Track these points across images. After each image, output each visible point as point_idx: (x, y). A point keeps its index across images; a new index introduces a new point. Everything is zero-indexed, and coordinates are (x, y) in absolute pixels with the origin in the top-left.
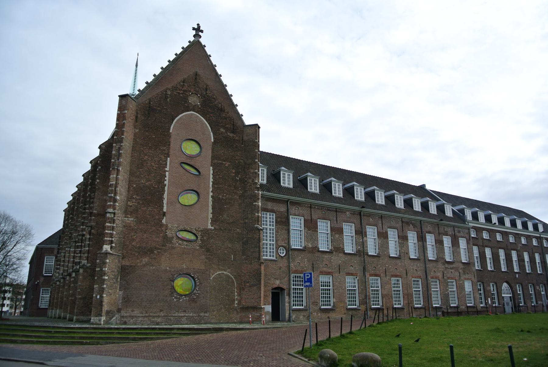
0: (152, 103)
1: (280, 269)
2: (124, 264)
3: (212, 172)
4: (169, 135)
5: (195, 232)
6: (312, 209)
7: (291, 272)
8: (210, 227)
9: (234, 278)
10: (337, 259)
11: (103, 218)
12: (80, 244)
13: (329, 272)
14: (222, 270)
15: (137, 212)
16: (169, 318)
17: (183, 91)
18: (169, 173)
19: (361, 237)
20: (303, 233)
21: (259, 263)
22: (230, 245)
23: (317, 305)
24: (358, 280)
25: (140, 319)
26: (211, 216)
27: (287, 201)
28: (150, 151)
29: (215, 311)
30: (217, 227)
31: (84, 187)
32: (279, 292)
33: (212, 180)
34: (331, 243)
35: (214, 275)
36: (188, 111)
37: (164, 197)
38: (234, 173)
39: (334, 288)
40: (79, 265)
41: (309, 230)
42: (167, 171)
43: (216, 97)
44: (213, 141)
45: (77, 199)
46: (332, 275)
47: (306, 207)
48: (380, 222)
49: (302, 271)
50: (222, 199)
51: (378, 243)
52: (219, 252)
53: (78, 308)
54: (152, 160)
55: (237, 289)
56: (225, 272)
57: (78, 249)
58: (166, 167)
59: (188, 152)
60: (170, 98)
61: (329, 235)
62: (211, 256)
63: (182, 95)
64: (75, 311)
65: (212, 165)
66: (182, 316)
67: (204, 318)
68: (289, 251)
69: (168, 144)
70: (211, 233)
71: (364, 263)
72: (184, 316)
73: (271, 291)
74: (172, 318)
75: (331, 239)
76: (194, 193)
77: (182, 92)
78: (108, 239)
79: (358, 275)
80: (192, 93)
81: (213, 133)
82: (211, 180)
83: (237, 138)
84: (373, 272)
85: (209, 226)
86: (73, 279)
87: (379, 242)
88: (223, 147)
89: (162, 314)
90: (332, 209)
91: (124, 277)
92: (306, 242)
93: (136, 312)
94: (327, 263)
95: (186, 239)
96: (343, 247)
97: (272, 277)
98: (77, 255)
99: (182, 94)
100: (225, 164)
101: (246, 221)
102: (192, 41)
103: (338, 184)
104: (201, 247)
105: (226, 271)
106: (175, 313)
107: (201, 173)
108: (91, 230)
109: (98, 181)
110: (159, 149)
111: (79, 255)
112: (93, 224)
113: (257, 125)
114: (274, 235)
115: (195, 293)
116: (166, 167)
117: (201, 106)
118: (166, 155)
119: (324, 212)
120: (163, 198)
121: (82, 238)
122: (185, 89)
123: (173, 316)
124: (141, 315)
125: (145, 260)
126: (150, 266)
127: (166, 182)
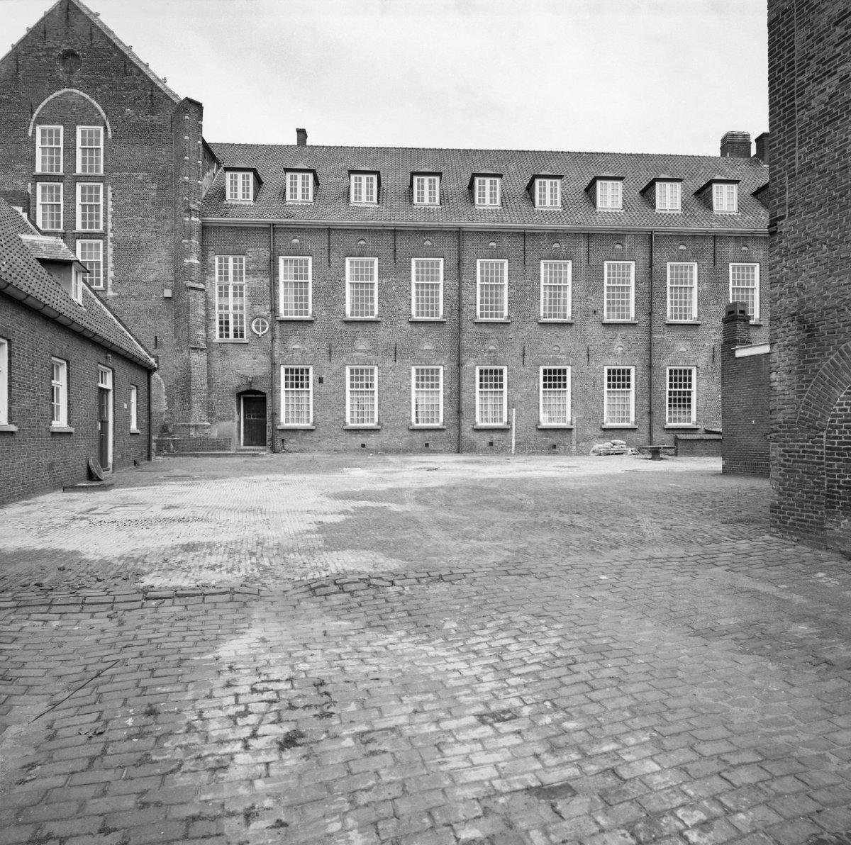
38: (154, 190)
88: (132, 144)
99: (44, 56)
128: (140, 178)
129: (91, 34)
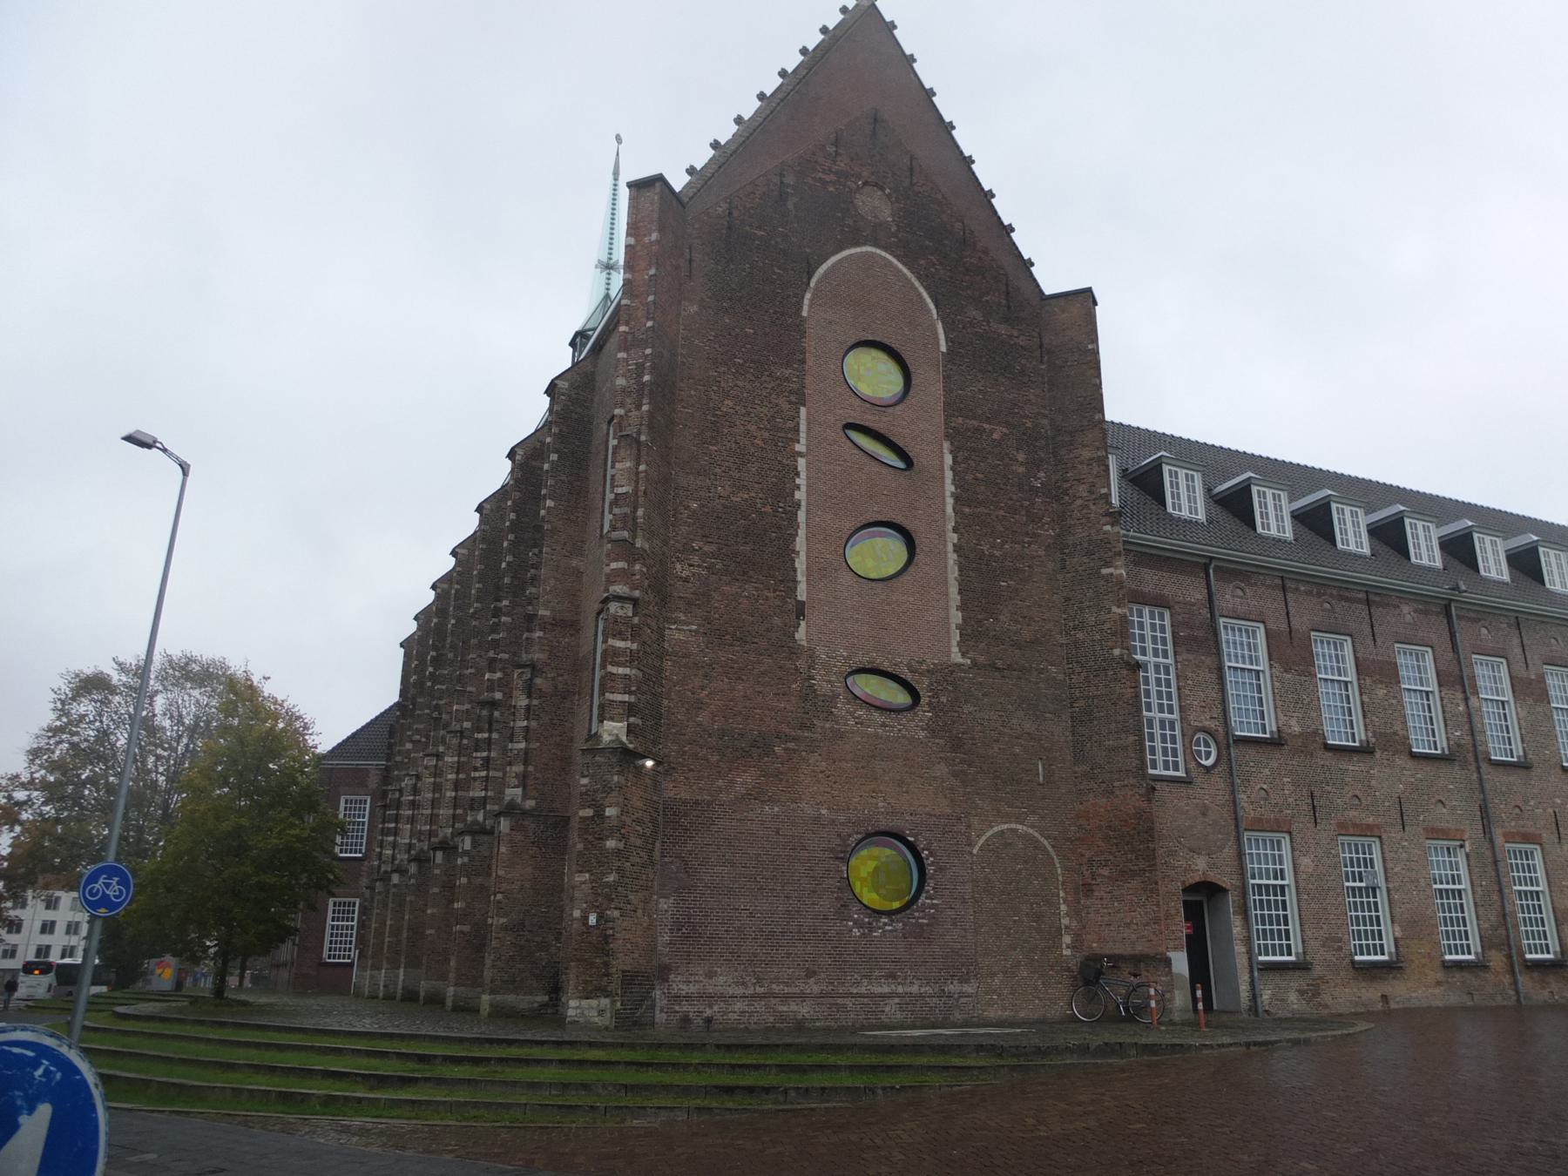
0: (736, 213)
1: (1204, 814)
2: (672, 794)
3: (948, 459)
4: (799, 327)
5: (908, 676)
6: (1289, 595)
7: (1243, 825)
8: (956, 657)
9: (1050, 849)
10: (1390, 778)
11: (571, 635)
12: (486, 735)
13: (1369, 826)
14: (1007, 818)
15: (708, 602)
16: (840, 1001)
17: (836, 173)
18: (808, 463)
19: (1460, 695)
20: (1266, 681)
21: (1143, 791)
22: (1029, 726)
23: (1340, 949)
24: (1467, 855)
25: (738, 1006)
26: (956, 617)
27: (1206, 568)
28: (739, 383)
29: (995, 974)
30: (982, 659)
31: (485, 546)
32: (1201, 903)
33: (953, 489)
34: (1365, 717)
35: (984, 838)
36: (857, 244)
37: (797, 549)
38: (1022, 463)
39: (1391, 886)
40: (485, 808)
41: (1286, 671)
42: (800, 454)
43: (944, 197)
44: (943, 349)
45: (456, 594)
46: (1380, 837)
47: (1268, 587)
48: (1516, 641)
49: (1277, 820)
50: (992, 555)
51: (1519, 720)
52: (996, 750)
53: (499, 963)
54: (749, 414)
55: (1066, 893)
56: (1019, 827)
57: (479, 754)
58: (798, 442)
59: (864, 389)
60: (796, 199)
61: (1354, 692)
62: (970, 766)
63: (831, 189)
64: (488, 973)
65: (947, 436)
66: (883, 996)
67: (962, 1000)
68: (1228, 747)
69: (799, 356)
70: (962, 679)
71: (1482, 791)
72: (891, 995)
73: (1182, 898)
74: (849, 1002)
75: (1362, 703)
76: (896, 537)
77: (833, 177)
78: (619, 697)
79: (1466, 837)
80: (865, 184)
81: (943, 322)
82: (950, 488)
83: (1022, 341)
84: (1513, 824)
85: (953, 655)
86: (466, 859)
87: (1521, 716)
88: (980, 371)
89: (813, 987)
90: (1354, 595)
91: (674, 845)
92: (1281, 716)
93: (721, 979)
94: (1358, 793)
95: (878, 704)
96: (1405, 732)
97: (1180, 842)
98: (477, 774)
99: (834, 183)
100: (992, 431)
101: (1080, 636)
102: (811, 48)
103: (1349, 508)
104: (933, 732)
105: (1022, 824)
106: (857, 984)
107: (915, 461)
108: (531, 679)
109: (549, 503)
110: (770, 375)
111: (484, 774)
112: (538, 656)
113: (1089, 291)
114: (1174, 690)
115: (923, 904)
116: (798, 442)
117: (898, 226)
118: (793, 398)
119: (1327, 606)
120: (794, 551)
121: (491, 715)
122: (842, 165)
123: (852, 996)
124: (740, 991)
125: (745, 779)
126: (763, 802)
127: (800, 495)
128: (995, 436)
129: (911, 169)
